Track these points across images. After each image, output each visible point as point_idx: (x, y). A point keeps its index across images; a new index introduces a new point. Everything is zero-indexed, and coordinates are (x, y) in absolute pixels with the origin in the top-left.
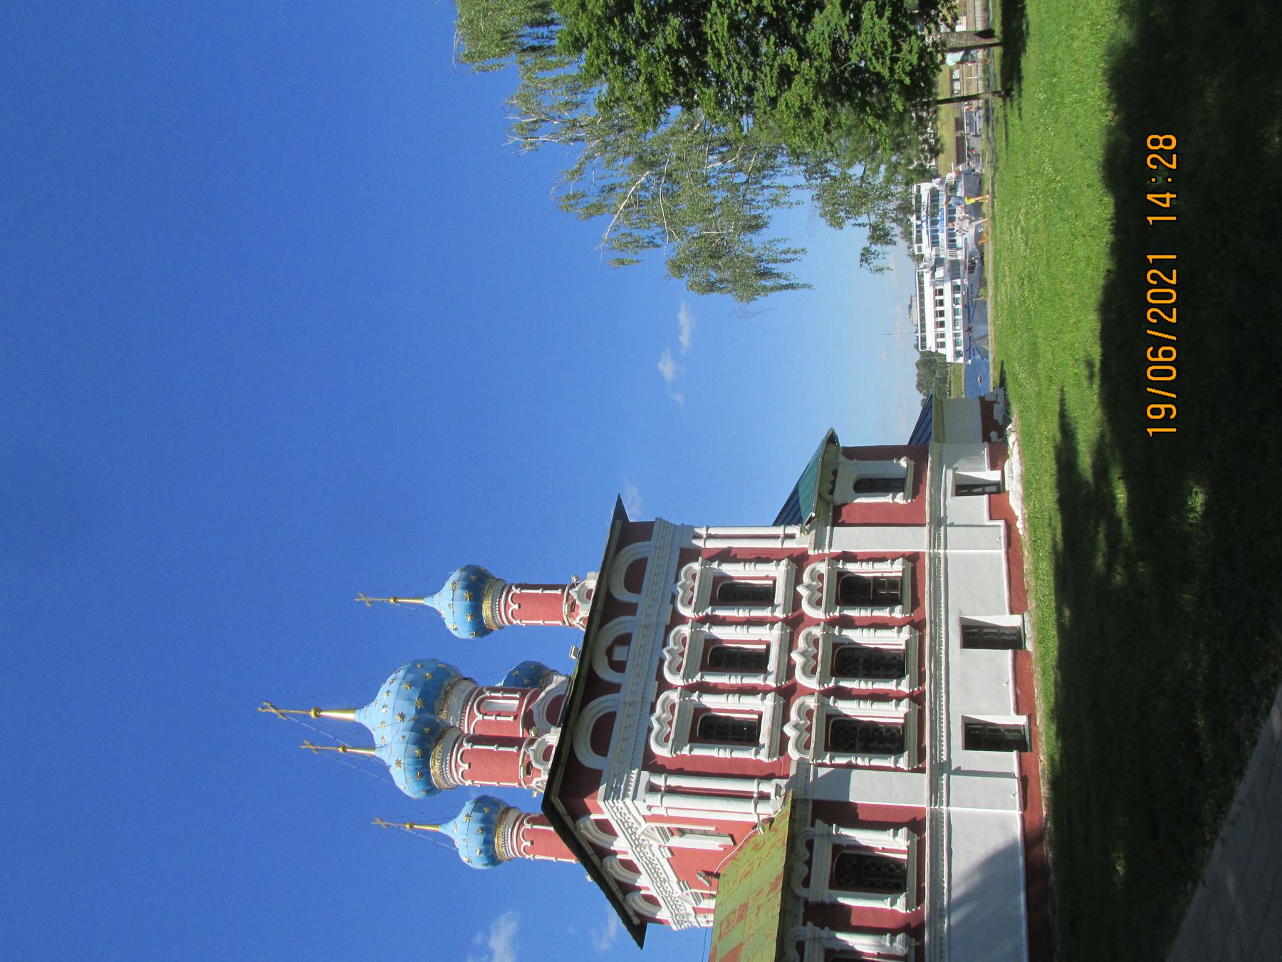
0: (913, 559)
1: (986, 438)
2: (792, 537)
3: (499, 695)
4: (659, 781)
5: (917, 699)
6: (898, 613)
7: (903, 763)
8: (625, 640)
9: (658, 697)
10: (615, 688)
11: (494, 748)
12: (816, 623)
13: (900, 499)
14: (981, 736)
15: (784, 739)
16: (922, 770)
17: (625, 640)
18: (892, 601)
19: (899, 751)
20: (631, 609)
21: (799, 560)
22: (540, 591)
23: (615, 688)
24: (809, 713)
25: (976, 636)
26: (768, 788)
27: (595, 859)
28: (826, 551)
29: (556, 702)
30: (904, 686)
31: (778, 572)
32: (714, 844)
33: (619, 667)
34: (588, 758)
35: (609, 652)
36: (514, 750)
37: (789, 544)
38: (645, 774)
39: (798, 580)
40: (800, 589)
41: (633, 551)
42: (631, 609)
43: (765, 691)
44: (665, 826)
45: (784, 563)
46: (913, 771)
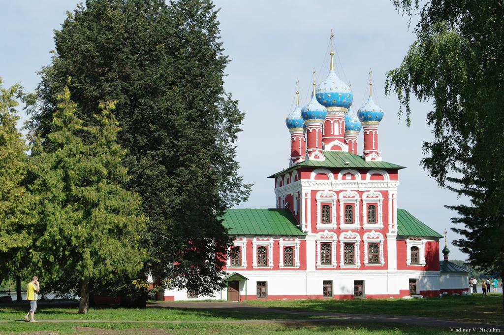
0: (385, 267)
1: (442, 291)
2: (393, 226)
3: (341, 127)
4: (309, 196)
5: (338, 268)
6: (366, 261)
7: (319, 263)
8: (353, 178)
9: (334, 191)
10: (336, 178)
11: (317, 140)
12: (361, 237)
13: (409, 261)
14: (328, 283)
15: (323, 231)
16: (316, 269)
17: (353, 178)
18: (370, 261)
19: (323, 263)
20: (364, 178)
21: (384, 231)
22: (374, 141)
23: (336, 178)
24: (332, 237)
25: (359, 283)
26: (309, 229)
27: (288, 171)
28: (388, 239)
29: (339, 148)
30: (342, 264)
31: (380, 225)
32: (295, 209)
33: (344, 178)
34: (313, 174)
35: (349, 173)
36: (317, 146)
37: (390, 228)
38: (310, 192)
39: (376, 231)
40: (373, 232)
41: (387, 176)
42: (364, 178)
43: (338, 224)
44: (298, 196)
45: (382, 226)
46: (316, 267)
